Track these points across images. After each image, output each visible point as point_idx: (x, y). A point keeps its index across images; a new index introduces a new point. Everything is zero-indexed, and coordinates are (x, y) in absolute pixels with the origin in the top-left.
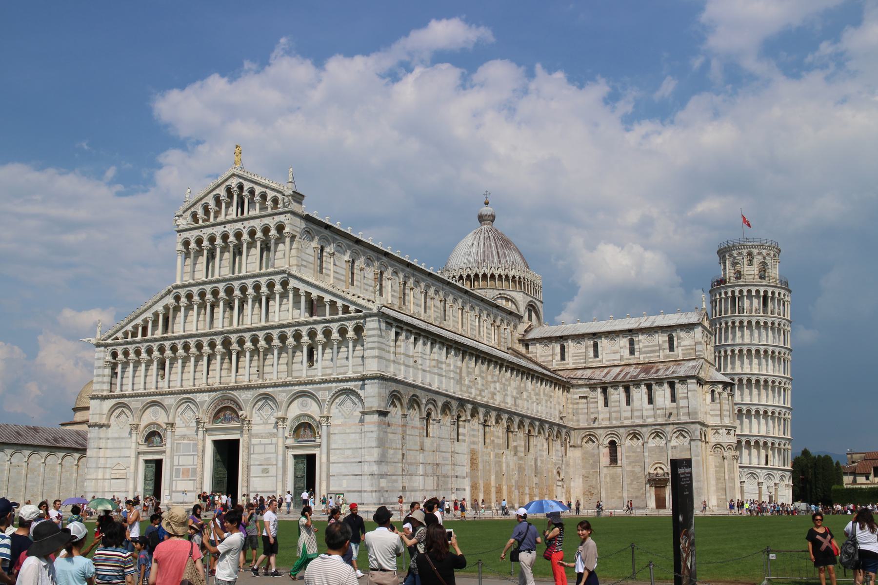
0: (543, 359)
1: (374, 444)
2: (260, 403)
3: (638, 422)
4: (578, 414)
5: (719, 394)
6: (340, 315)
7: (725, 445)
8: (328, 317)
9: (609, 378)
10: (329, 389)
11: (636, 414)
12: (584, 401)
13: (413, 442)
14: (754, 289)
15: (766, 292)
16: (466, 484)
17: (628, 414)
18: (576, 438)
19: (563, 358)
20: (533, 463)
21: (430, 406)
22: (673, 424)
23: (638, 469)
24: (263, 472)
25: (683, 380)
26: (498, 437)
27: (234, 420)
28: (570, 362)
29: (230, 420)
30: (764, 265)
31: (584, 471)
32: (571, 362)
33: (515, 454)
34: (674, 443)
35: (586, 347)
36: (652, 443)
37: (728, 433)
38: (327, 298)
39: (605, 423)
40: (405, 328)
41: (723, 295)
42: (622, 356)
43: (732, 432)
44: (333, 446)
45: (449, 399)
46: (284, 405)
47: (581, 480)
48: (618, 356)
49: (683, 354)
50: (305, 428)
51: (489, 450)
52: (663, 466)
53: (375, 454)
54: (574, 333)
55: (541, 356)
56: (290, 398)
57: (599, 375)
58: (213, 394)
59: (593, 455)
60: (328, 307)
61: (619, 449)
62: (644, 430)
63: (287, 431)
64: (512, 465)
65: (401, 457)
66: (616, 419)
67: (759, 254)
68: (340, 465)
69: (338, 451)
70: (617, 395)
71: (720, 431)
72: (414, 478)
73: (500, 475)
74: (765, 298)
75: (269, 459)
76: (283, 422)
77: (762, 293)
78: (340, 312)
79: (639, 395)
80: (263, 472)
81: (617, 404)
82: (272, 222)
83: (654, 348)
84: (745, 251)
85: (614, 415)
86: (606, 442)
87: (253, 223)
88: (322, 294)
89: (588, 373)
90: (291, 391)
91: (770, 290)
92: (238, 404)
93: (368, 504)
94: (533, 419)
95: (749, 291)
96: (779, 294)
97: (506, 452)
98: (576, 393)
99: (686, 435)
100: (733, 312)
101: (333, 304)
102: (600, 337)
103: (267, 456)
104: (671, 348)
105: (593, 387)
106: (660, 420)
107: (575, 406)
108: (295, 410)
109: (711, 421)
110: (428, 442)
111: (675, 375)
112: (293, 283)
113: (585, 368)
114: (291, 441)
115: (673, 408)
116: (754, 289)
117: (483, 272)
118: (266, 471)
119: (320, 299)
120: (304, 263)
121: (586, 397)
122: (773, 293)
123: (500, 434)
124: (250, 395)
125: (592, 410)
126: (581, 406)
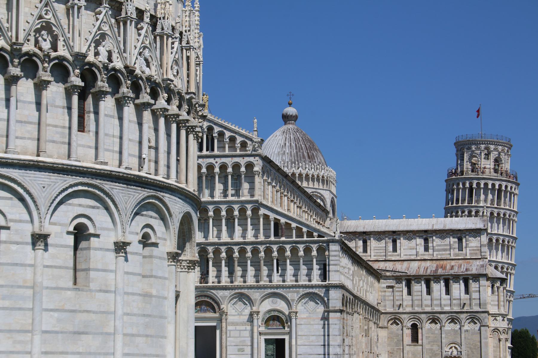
1: (337, 333)
2: (235, 300)
5: (498, 288)
6: (305, 239)
7: (501, 329)
8: (294, 239)
12: (391, 290)
14: (490, 183)
15: (500, 186)
18: (384, 320)
22: (467, 312)
23: (436, 348)
25: (476, 277)
27: (209, 311)
29: (205, 311)
30: (497, 161)
31: (389, 348)
32: (373, 254)
36: (449, 327)
37: (503, 320)
38: (294, 225)
39: (409, 309)
41: (461, 186)
43: (505, 319)
44: (299, 333)
46: (258, 302)
47: (387, 355)
48: (414, 252)
49: (471, 254)
50: (275, 319)
52: (457, 346)
54: (376, 230)
56: (262, 298)
57: (401, 267)
59: (397, 335)
60: (294, 231)
61: (420, 331)
62: (442, 316)
63: (260, 320)
66: (418, 306)
67: (495, 149)
68: (306, 347)
69: (304, 337)
70: (419, 288)
71: (498, 318)
74: (500, 190)
75: (244, 341)
76: (257, 315)
77: (497, 187)
78: (305, 236)
79: (438, 288)
82: (243, 161)
83: (446, 247)
84: (483, 146)
85: (416, 302)
86: (409, 325)
87: (224, 160)
88: (278, 217)
91: (504, 184)
92: (214, 300)
95: (486, 185)
96: (511, 188)
98: (384, 283)
100: (470, 201)
101: (299, 230)
102: (399, 235)
103: (243, 339)
104: (460, 249)
105: (398, 279)
106: (456, 309)
107: (383, 293)
108: (267, 306)
109: (493, 310)
111: (469, 273)
112: (262, 211)
114: (262, 329)
115: (467, 299)
116: (490, 183)
119: (288, 225)
121: (392, 287)
122: (506, 187)
124: (227, 293)
125: (397, 298)
126: (387, 294)
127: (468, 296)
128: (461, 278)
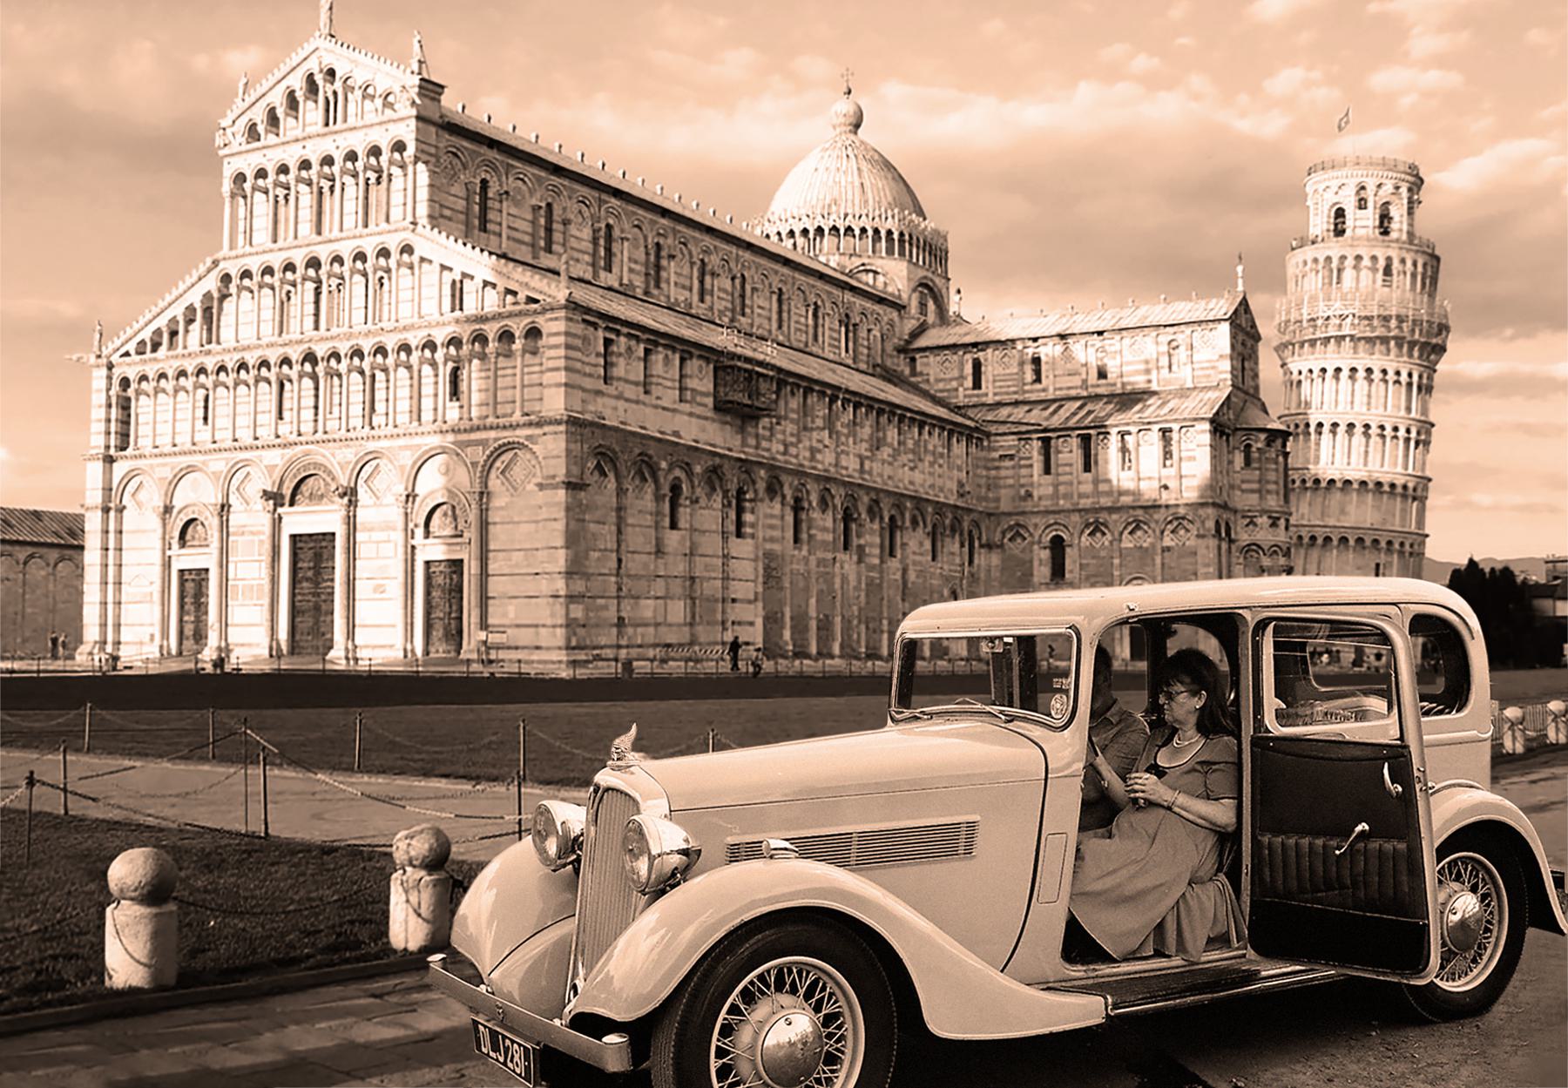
0: (941, 386)
1: (560, 542)
3: (1105, 501)
4: (997, 487)
9: (1056, 422)
10: (483, 443)
11: (1103, 487)
12: (1008, 463)
13: (639, 537)
16: (756, 614)
17: (1087, 488)
19: (977, 384)
20: (898, 576)
21: (678, 473)
24: (375, 591)
26: (825, 529)
28: (989, 392)
33: (860, 561)
34: (1168, 541)
35: (1022, 364)
37: (1274, 525)
39: (1046, 504)
40: (625, 330)
42: (1085, 381)
45: (717, 460)
48: (1077, 381)
51: (804, 553)
53: (560, 560)
55: (938, 380)
58: (289, 452)
61: (1068, 550)
64: (852, 578)
65: (615, 565)
66: (1065, 496)
69: (500, 555)
71: (1259, 521)
72: (643, 602)
73: (827, 596)
80: (375, 591)
81: (1067, 469)
85: (1062, 489)
86: (1047, 539)
89: (1019, 413)
90: (419, 446)
93: (548, 649)
94: (899, 499)
97: (840, 556)
99: (1190, 526)
107: (993, 473)
110: (673, 539)
113: (1016, 403)
117: (831, 223)
118: (379, 589)
120: (447, 213)
121: (1011, 457)
123: (829, 524)
126: (1003, 473)
127: (1172, 471)
128: (1156, 428)
